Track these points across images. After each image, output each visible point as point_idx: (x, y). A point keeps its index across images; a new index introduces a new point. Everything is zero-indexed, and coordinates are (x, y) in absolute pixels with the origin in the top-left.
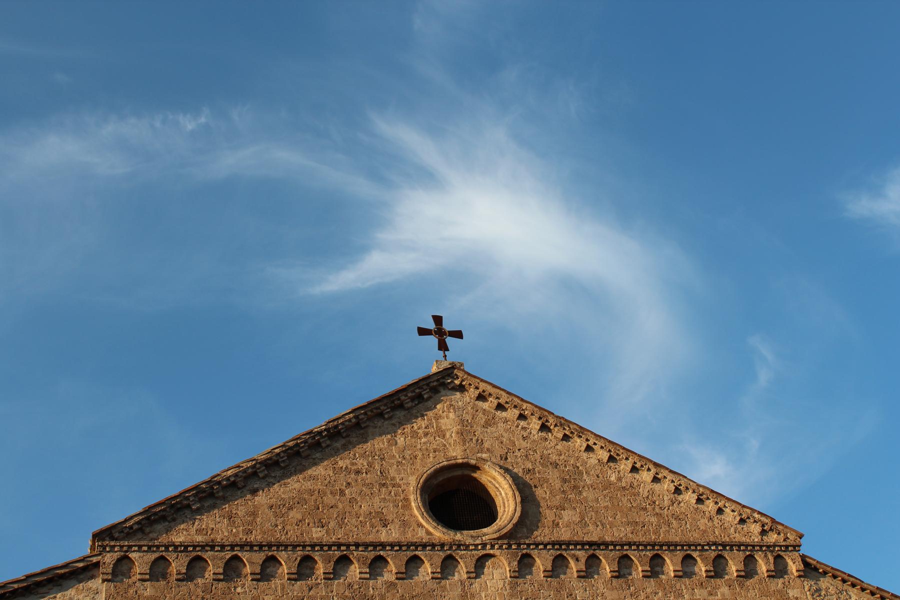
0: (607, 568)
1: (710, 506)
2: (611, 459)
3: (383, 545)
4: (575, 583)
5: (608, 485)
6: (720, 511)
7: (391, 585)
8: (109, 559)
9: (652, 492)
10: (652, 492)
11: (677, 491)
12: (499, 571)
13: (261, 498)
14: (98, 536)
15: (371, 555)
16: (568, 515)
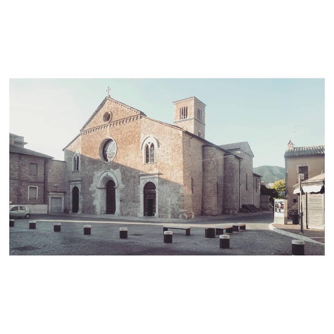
0: (118, 123)
1: (131, 110)
2: (122, 106)
3: (99, 126)
4: (116, 126)
5: (122, 110)
6: (132, 110)
7: (100, 131)
8: (81, 133)
9: (125, 110)
10: (125, 110)
11: (128, 109)
12: (108, 127)
13: (92, 123)
14: (80, 131)
15: (98, 127)
16: (116, 116)
